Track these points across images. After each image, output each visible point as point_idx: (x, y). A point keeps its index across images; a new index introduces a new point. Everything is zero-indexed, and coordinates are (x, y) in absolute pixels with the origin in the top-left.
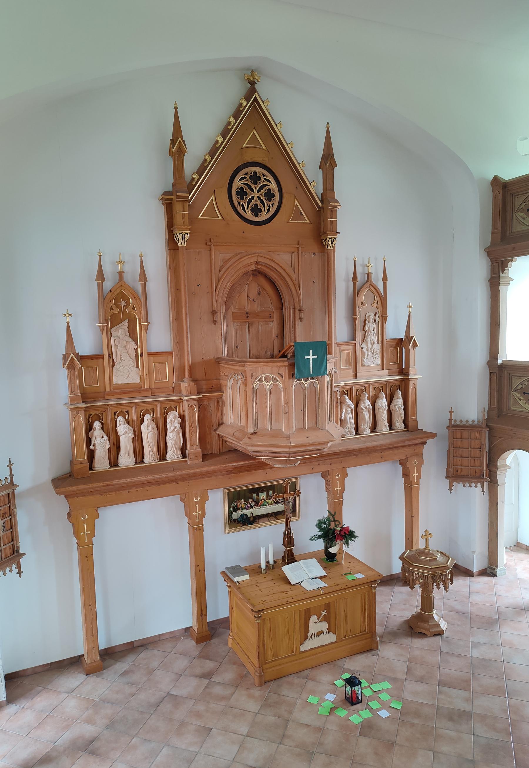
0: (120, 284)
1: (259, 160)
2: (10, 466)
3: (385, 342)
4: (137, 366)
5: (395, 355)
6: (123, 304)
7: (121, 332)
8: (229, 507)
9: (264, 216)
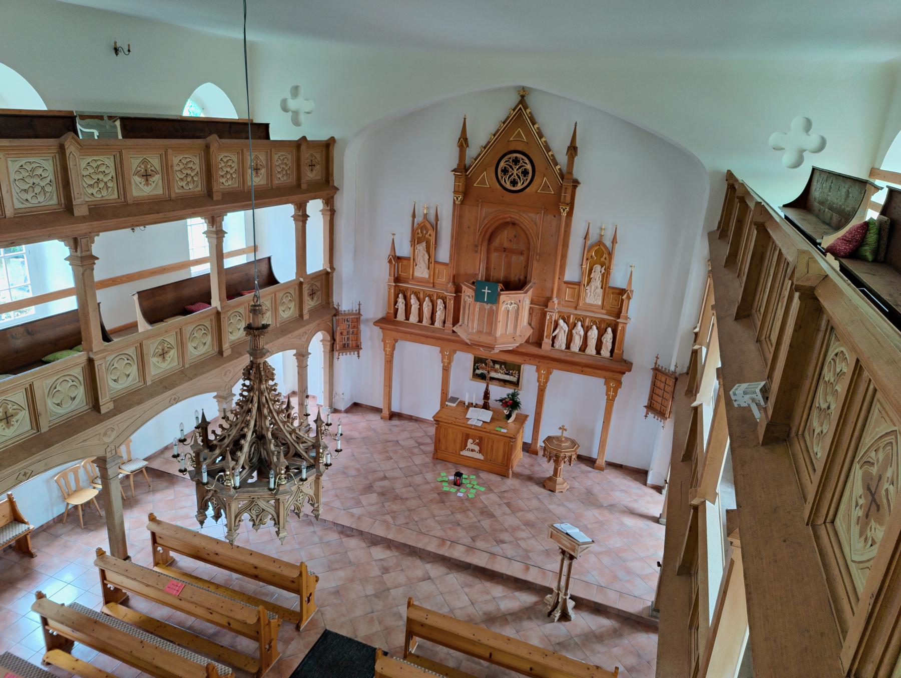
9: (519, 186)
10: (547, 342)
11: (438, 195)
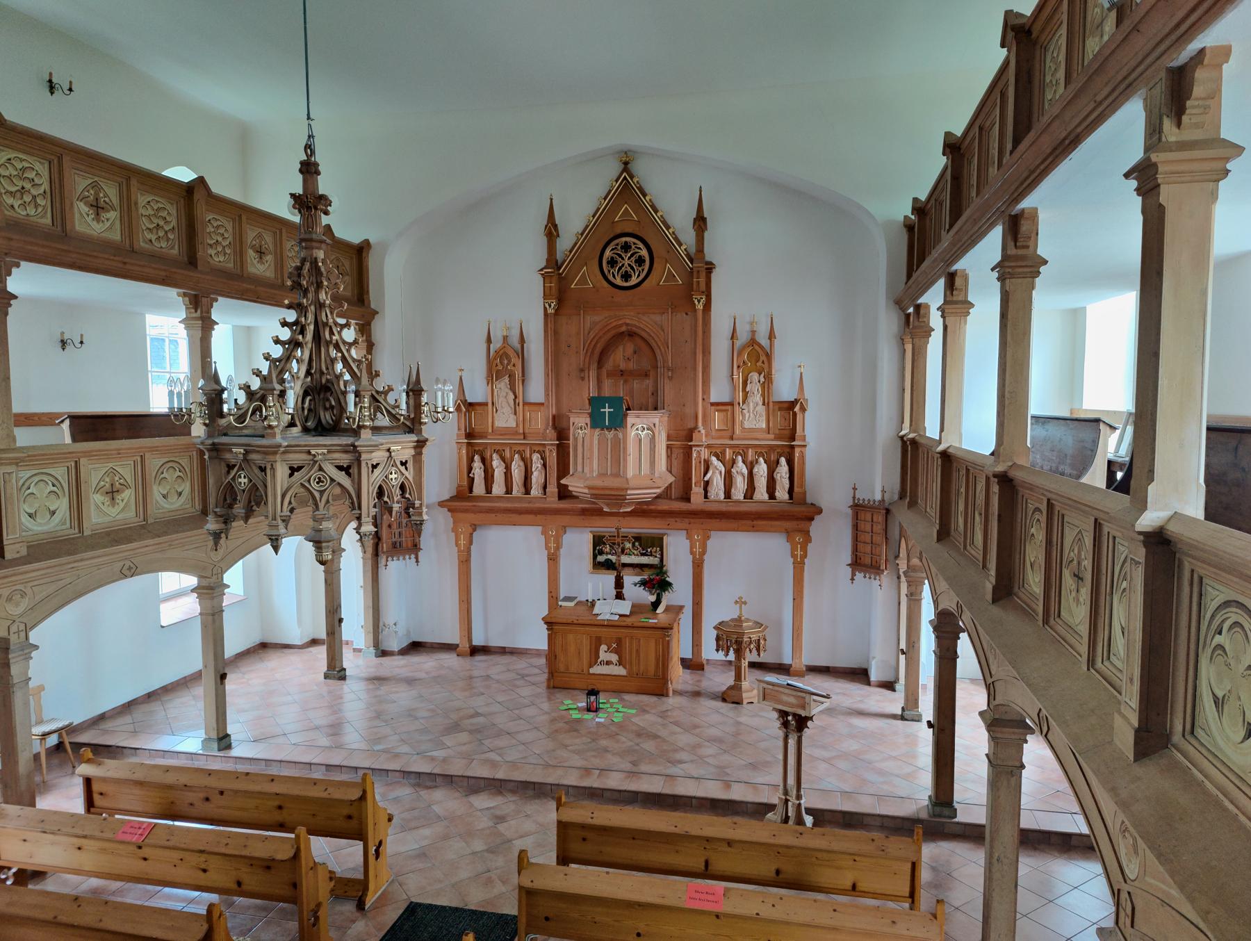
9: (634, 280)
10: (697, 491)
11: (522, 308)
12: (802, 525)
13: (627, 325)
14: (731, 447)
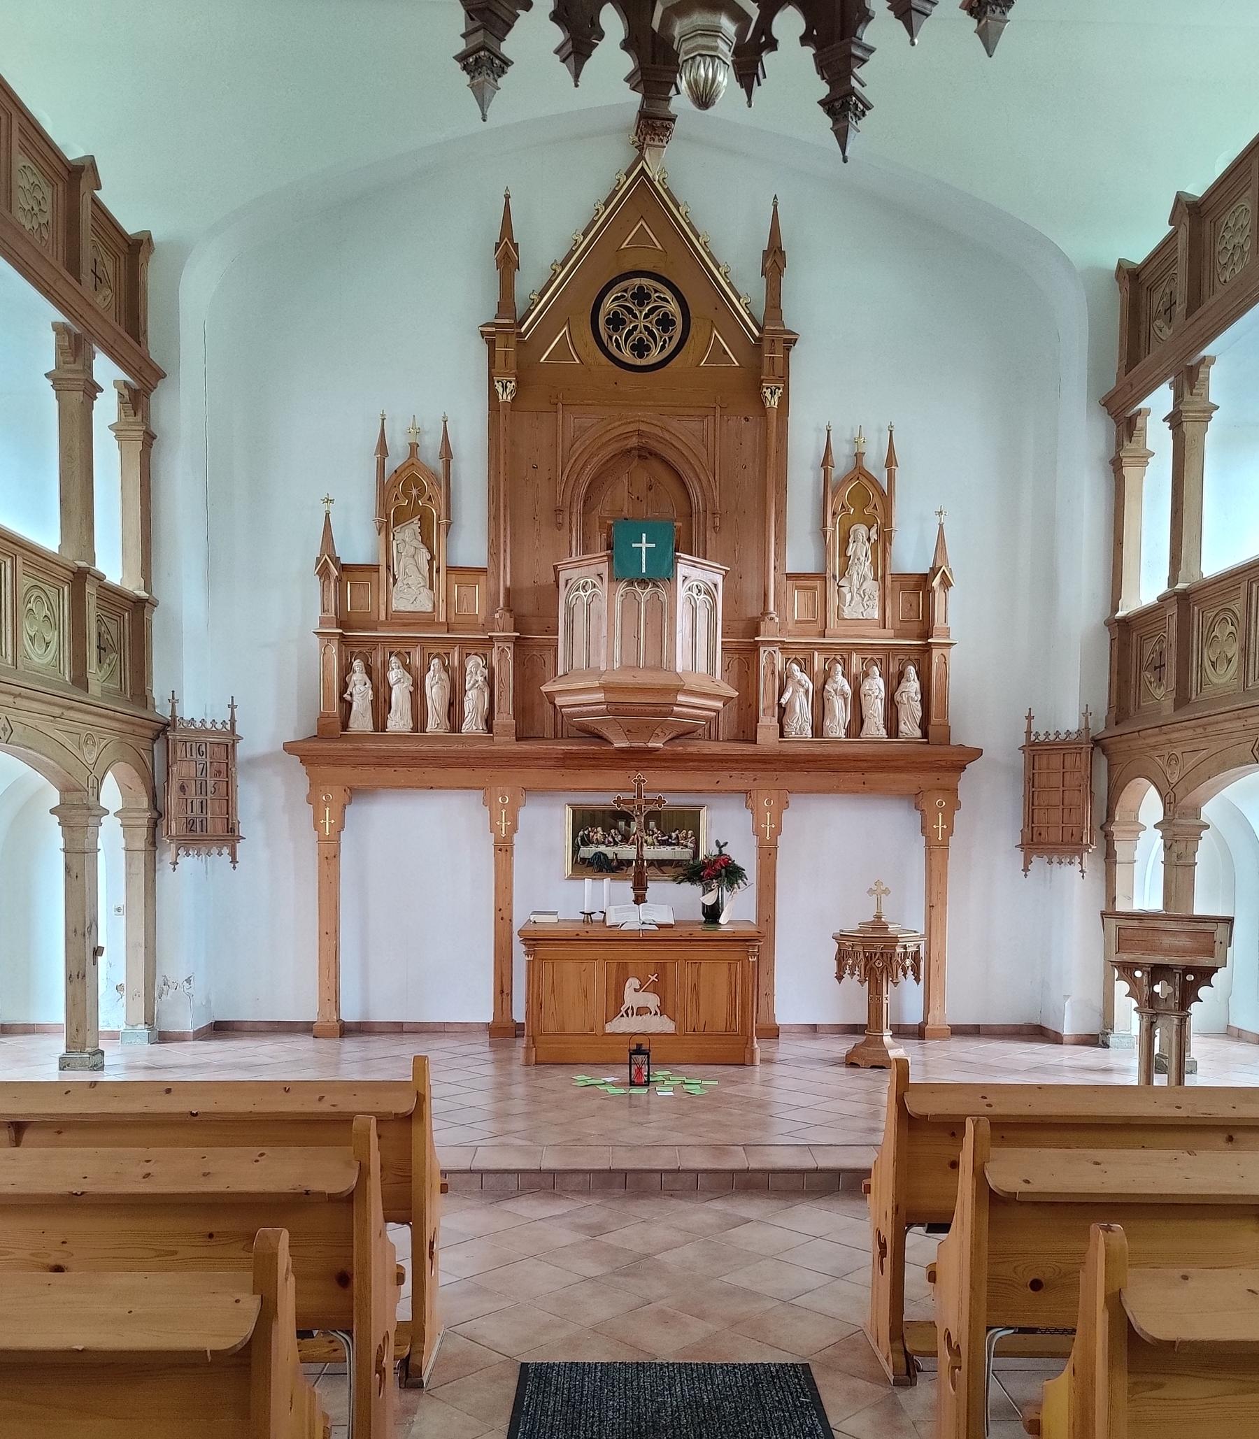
0: (410, 461)
1: (647, 267)
2: (232, 707)
3: (888, 578)
4: (431, 588)
5: (914, 607)
6: (414, 492)
7: (408, 534)
8: (575, 837)
9: (654, 356)
10: (767, 722)
11: (445, 396)
12: (946, 779)
13: (640, 434)
14: (824, 649)
